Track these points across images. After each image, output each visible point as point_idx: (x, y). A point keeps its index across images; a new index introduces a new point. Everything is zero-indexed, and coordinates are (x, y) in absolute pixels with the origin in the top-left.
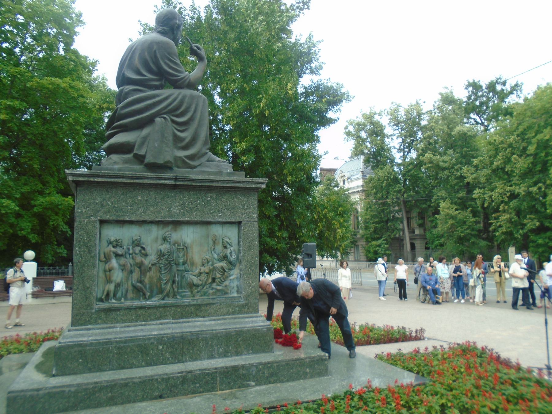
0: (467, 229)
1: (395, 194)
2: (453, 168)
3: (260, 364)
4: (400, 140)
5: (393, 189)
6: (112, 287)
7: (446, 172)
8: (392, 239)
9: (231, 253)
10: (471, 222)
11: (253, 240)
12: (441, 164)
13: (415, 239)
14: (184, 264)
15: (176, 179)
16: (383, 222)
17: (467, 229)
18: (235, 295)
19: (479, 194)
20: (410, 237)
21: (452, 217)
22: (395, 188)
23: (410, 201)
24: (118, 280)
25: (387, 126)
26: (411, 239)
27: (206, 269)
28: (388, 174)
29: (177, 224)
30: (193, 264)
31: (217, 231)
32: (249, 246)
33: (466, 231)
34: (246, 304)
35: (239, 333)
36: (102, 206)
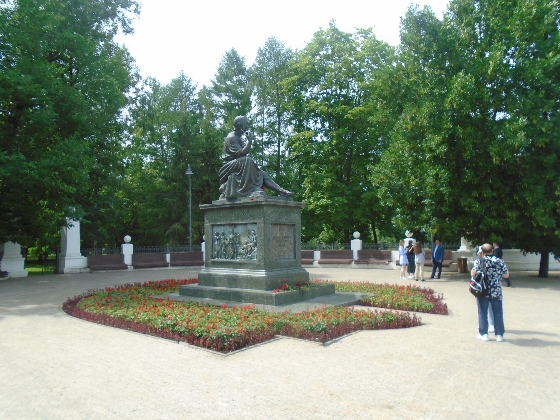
3: (246, 292)
6: (216, 253)
9: (254, 239)
11: (262, 232)
14: (238, 243)
15: (230, 205)
18: (255, 260)
24: (218, 250)
27: (245, 246)
29: (235, 225)
30: (241, 244)
31: (250, 227)
32: (260, 235)
34: (259, 265)
35: (252, 278)
36: (211, 218)
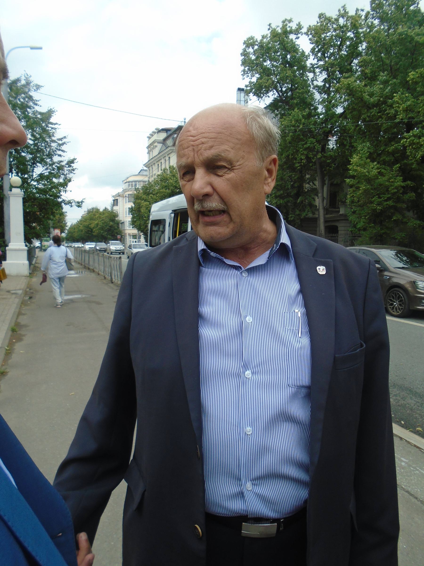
0: (388, 199)
1: (305, 152)
2: (385, 102)
4: (324, 75)
5: (303, 145)
7: (374, 111)
8: (302, 220)
10: (396, 188)
12: (366, 96)
13: (338, 221)
16: (288, 195)
17: (388, 199)
19: (412, 138)
20: (325, 218)
21: (369, 180)
22: (306, 143)
23: (329, 165)
25: (311, 54)
26: (326, 221)
28: (297, 121)
33: (386, 203)
